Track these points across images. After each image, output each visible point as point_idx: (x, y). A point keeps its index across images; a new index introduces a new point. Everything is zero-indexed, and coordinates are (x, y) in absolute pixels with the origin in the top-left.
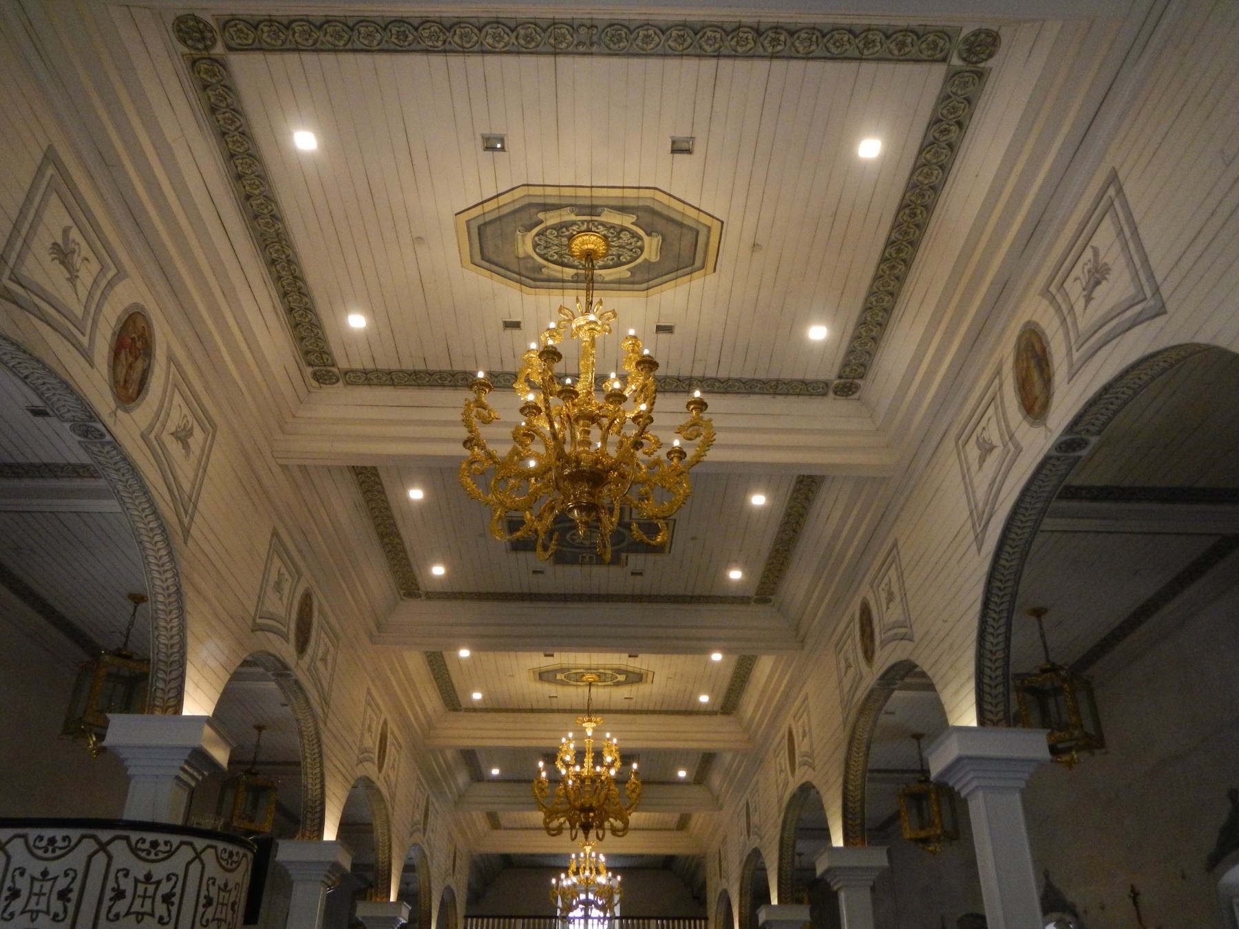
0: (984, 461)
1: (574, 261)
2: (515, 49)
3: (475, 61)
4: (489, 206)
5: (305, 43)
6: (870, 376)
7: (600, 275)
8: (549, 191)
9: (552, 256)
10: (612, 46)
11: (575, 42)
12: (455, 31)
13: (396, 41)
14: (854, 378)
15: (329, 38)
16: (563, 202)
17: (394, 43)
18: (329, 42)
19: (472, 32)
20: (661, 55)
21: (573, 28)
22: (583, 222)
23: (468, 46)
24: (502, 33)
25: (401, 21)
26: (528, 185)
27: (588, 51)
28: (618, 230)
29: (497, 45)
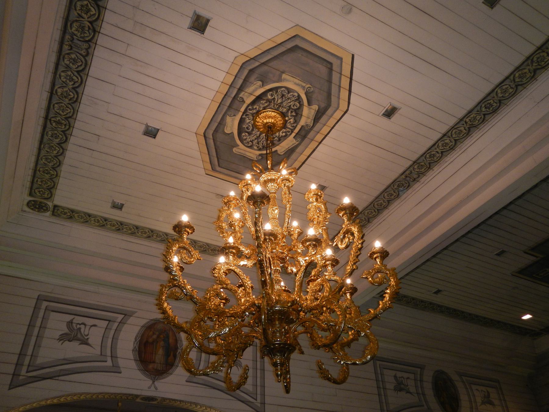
0: (69, 341)
1: (260, 107)
2: (433, 148)
3: (444, 129)
4: (345, 82)
5: (538, 56)
6: (54, 220)
7: (234, 115)
8: (332, 122)
9: (272, 95)
10: (399, 183)
11: (413, 171)
12: (466, 130)
13: (490, 102)
14: (53, 212)
15: (525, 71)
16: (318, 126)
17: (490, 100)
18: (525, 69)
19: (458, 137)
20: (379, 196)
21: (420, 173)
22: (295, 128)
23: (454, 131)
24: (445, 148)
25: (495, 111)
26: (346, 112)
27: (405, 174)
28: (275, 142)
29: (442, 142)
